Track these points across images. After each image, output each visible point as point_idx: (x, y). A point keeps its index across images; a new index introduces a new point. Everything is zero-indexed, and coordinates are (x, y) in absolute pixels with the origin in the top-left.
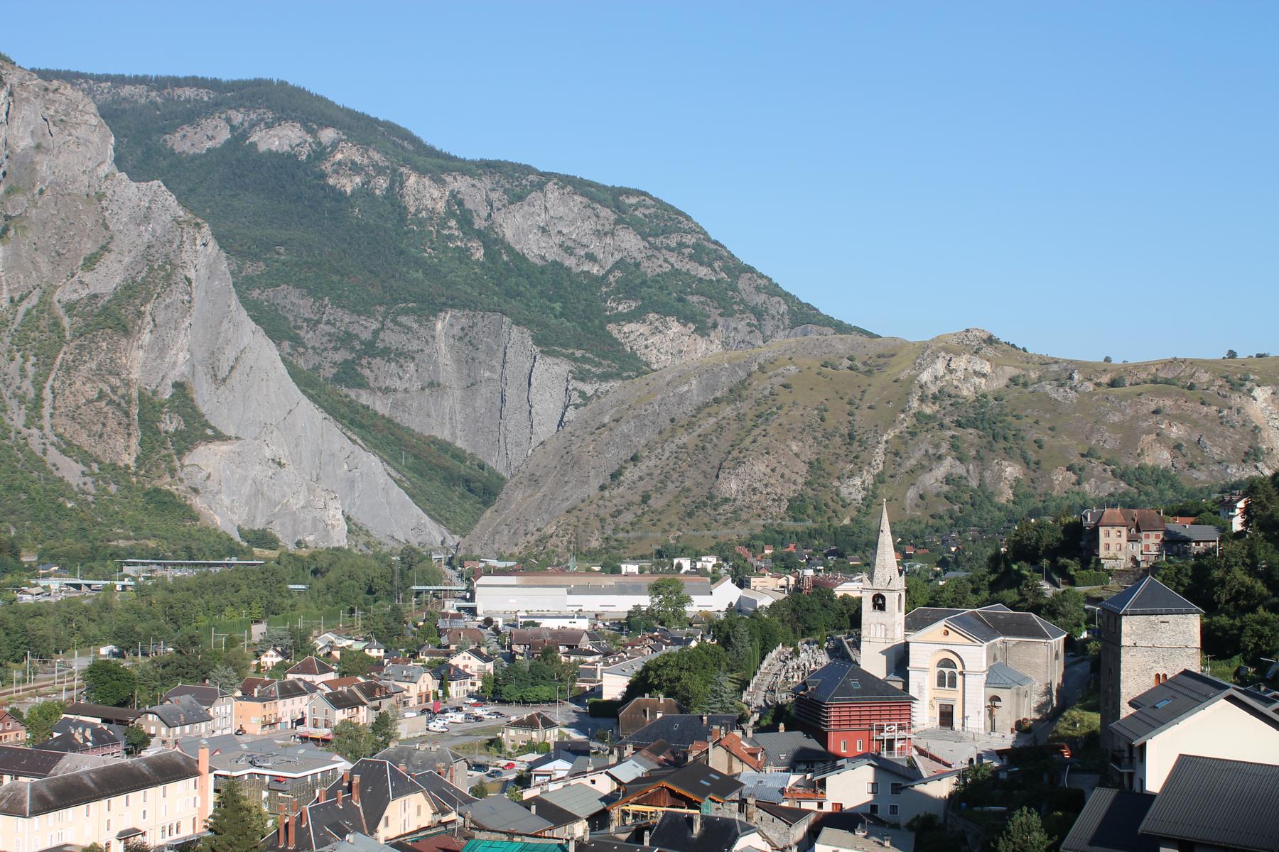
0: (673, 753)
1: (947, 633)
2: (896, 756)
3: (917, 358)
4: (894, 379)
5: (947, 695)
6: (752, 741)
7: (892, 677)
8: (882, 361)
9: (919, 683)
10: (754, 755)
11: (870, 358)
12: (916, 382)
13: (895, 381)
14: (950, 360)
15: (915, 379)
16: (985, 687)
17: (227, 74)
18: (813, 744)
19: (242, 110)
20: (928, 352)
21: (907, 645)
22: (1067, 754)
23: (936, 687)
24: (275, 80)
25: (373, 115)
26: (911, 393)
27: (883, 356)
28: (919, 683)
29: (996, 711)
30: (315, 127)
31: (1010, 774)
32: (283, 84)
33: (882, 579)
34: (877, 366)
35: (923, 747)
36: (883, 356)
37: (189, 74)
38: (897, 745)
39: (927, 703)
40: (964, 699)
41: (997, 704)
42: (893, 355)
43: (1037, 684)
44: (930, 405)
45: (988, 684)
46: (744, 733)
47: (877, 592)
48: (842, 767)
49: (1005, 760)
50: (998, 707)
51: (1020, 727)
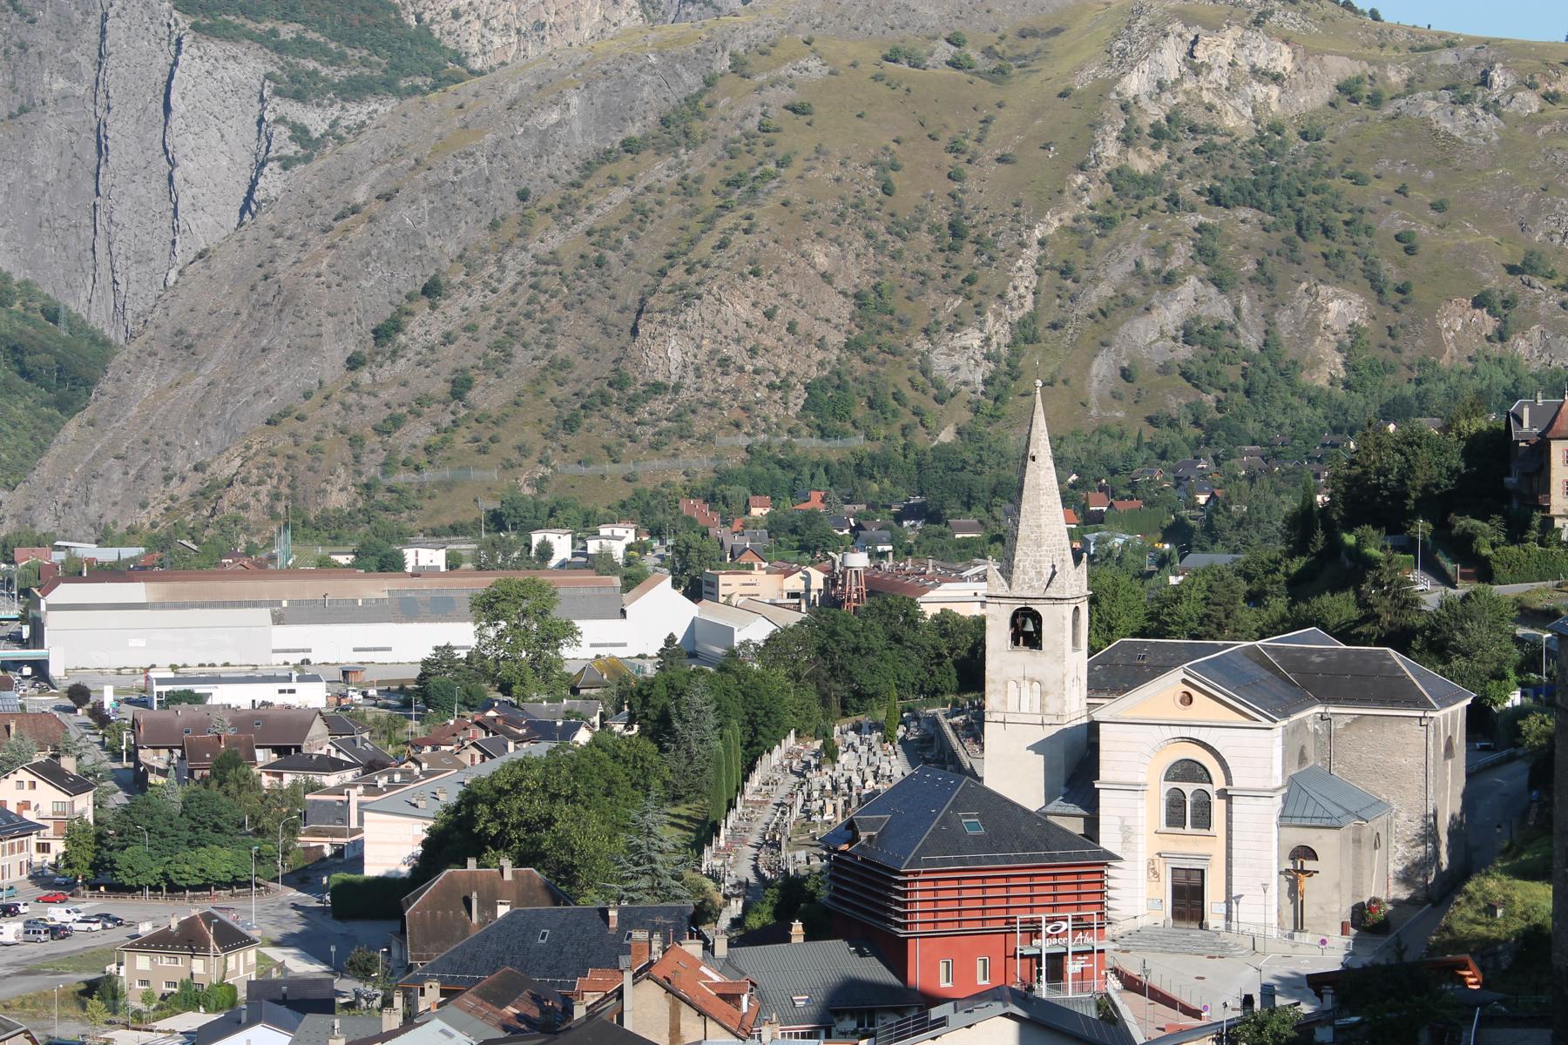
0: (537, 999)
1: (1187, 699)
2: (1069, 994)
3: (1116, 37)
4: (1060, 88)
5: (1191, 845)
6: (727, 965)
7: (1058, 805)
8: (1030, 45)
9: (1123, 819)
10: (732, 998)
11: (1002, 38)
12: (1113, 96)
13: (1061, 95)
14: (1195, 42)
15: (1112, 90)
16: (1280, 826)
18: (873, 970)
20: (1142, 22)
21: (1093, 728)
22: (1473, 980)
23: (1164, 828)
26: (1101, 124)
27: (1034, 34)
28: (1123, 819)
29: (1306, 883)
31: (1338, 1031)
33: (1032, 573)
34: (1020, 57)
35: (1134, 970)
36: (1034, 34)
38: (1072, 967)
39: (1142, 866)
41: (1309, 865)
42: (1057, 31)
43: (1403, 816)
44: (1146, 150)
45: (1286, 819)
46: (708, 947)
47: (1020, 604)
48: (942, 1022)
49: (1328, 999)
50: (1309, 873)
51: (1363, 920)
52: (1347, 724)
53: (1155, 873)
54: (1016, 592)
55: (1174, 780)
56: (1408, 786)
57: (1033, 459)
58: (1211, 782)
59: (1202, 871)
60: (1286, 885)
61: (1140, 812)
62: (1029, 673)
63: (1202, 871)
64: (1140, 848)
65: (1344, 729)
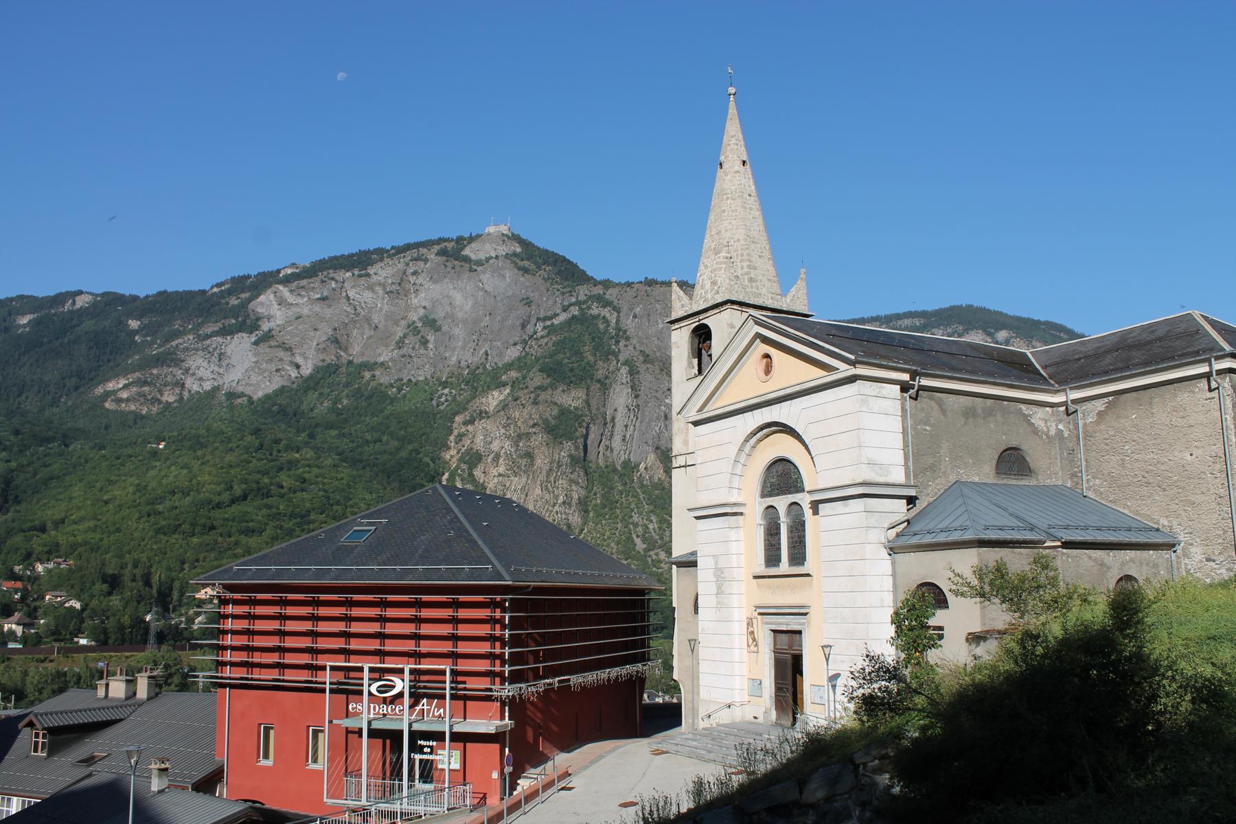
17: (931, 306)
19: (942, 327)
24: (964, 305)
25: (1035, 318)
30: (992, 331)
32: (970, 307)
33: (708, 286)
37: (906, 310)
39: (740, 628)
43: (1197, 553)
47: (692, 324)
52: (1100, 414)
53: (754, 640)
55: (771, 495)
56: (1200, 498)
59: (800, 632)
61: (734, 548)
63: (800, 632)
64: (735, 601)
65: (1098, 423)
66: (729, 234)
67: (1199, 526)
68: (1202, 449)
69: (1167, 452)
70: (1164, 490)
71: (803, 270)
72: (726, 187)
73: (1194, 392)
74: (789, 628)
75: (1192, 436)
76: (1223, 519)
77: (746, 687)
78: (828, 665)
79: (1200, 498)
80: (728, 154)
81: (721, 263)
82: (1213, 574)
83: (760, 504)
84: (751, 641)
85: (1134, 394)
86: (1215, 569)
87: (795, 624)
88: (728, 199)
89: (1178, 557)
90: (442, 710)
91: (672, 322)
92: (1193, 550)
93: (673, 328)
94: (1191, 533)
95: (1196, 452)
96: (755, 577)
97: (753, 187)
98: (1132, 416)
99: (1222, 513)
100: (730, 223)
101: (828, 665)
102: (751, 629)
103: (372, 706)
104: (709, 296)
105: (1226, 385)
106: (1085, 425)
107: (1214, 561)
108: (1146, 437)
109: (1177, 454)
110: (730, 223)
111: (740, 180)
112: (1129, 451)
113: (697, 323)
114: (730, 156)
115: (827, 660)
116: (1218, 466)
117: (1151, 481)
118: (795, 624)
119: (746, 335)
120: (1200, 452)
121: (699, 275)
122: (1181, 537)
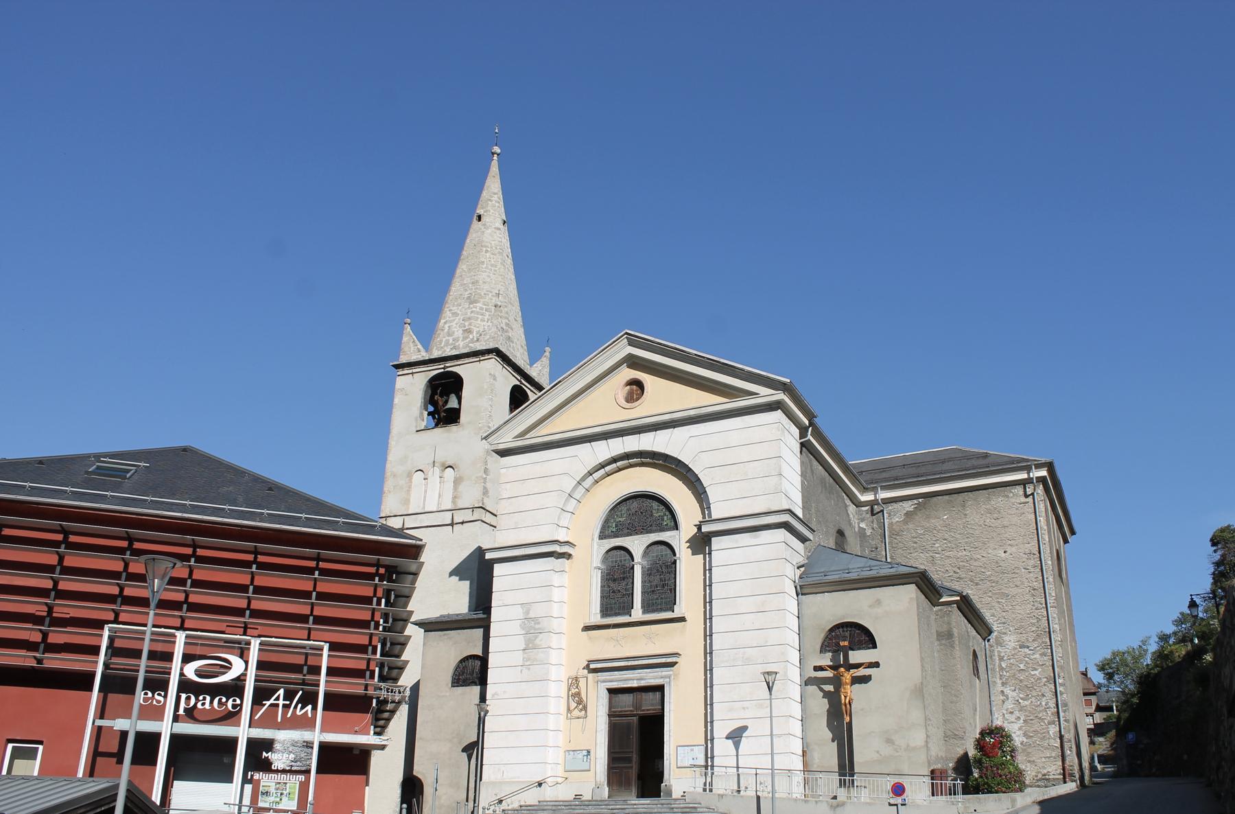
9: (526, 606)
33: (459, 333)
39: (558, 691)
40: (708, 652)
43: (1011, 641)
52: (908, 514)
54: (436, 354)
55: (616, 536)
56: (1014, 591)
57: (479, 218)
58: (676, 527)
59: (660, 689)
60: (820, 706)
61: (556, 594)
62: (442, 456)
64: (554, 657)
65: (905, 522)
66: (486, 287)
67: (1013, 616)
68: (1016, 547)
69: (980, 549)
70: (977, 584)
71: (548, 349)
72: (484, 239)
73: (1008, 497)
74: (643, 683)
75: (1006, 535)
76: (1036, 609)
77: (561, 761)
78: (771, 694)
79: (1014, 591)
80: (489, 208)
81: (478, 313)
82: (1027, 659)
83: (599, 546)
84: (573, 705)
85: (946, 497)
86: (1029, 654)
87: (655, 678)
88: (487, 251)
89: (990, 646)
90: (309, 707)
91: (398, 367)
92: (1006, 638)
93: (399, 373)
94: (1004, 623)
95: (1009, 550)
96: (587, 628)
97: (510, 250)
98: (942, 516)
99: (1035, 603)
100: (489, 276)
101: (771, 694)
102: (573, 691)
103: (184, 696)
104: (461, 344)
105: (1039, 491)
106: (891, 524)
107: (1028, 647)
108: (958, 536)
109: (990, 551)
110: (489, 276)
111: (500, 238)
112: (940, 549)
113: (442, 370)
114: (492, 211)
115: (770, 689)
116: (1032, 562)
117: (963, 576)
118: (655, 678)
119: (612, 356)
120: (1014, 549)
121: (442, 321)
122: (995, 628)
